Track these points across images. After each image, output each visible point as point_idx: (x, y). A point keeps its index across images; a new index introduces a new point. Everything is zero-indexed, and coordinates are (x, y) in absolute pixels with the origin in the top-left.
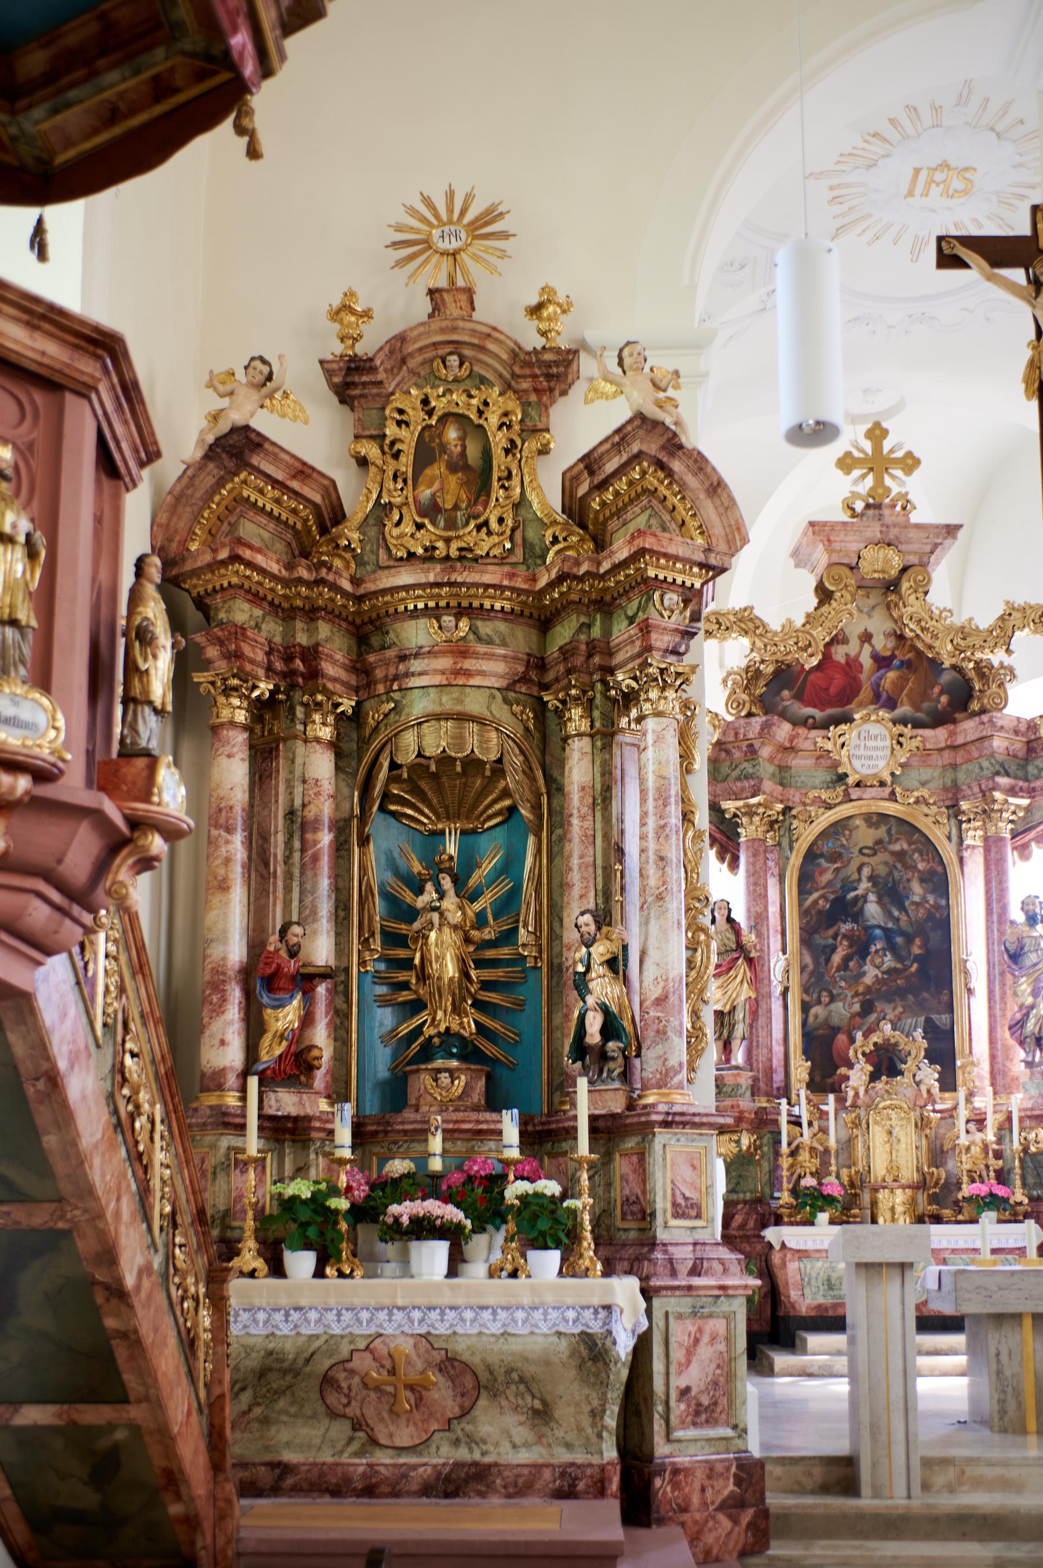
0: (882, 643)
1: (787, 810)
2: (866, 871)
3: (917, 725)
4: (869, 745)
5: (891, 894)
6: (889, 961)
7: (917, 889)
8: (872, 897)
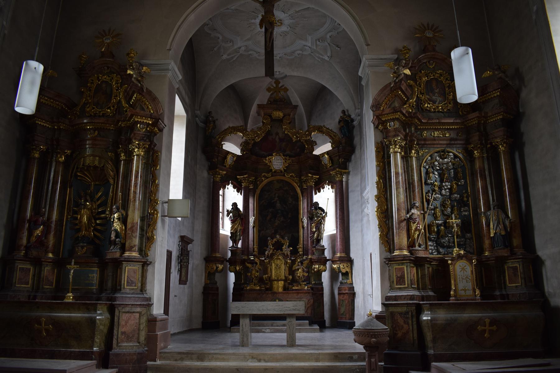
1: (256, 178)
2: (277, 195)
3: (290, 156)
4: (277, 162)
8: (278, 202)
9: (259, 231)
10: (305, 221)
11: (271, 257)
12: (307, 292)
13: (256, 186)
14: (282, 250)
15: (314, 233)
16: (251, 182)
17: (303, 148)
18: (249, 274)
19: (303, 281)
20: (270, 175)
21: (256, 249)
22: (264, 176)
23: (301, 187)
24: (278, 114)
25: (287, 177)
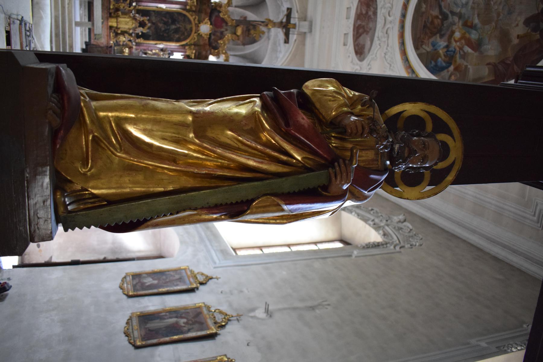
0: (226, 32)
2: (181, 26)
3: (210, 38)
4: (205, 28)
5: (177, 31)
6: (163, 29)
7: (177, 36)
9: (154, 11)
10: (161, 46)
11: (134, 18)
12: (108, 43)
13: (188, 11)
14: (139, 26)
15: (151, 51)
16: (191, 7)
17: (215, 48)
18: (122, 1)
19: (116, 41)
20: (197, 22)
21: (140, 8)
22: (195, 18)
23: (186, 45)
24: (239, 31)
25: (194, 35)
